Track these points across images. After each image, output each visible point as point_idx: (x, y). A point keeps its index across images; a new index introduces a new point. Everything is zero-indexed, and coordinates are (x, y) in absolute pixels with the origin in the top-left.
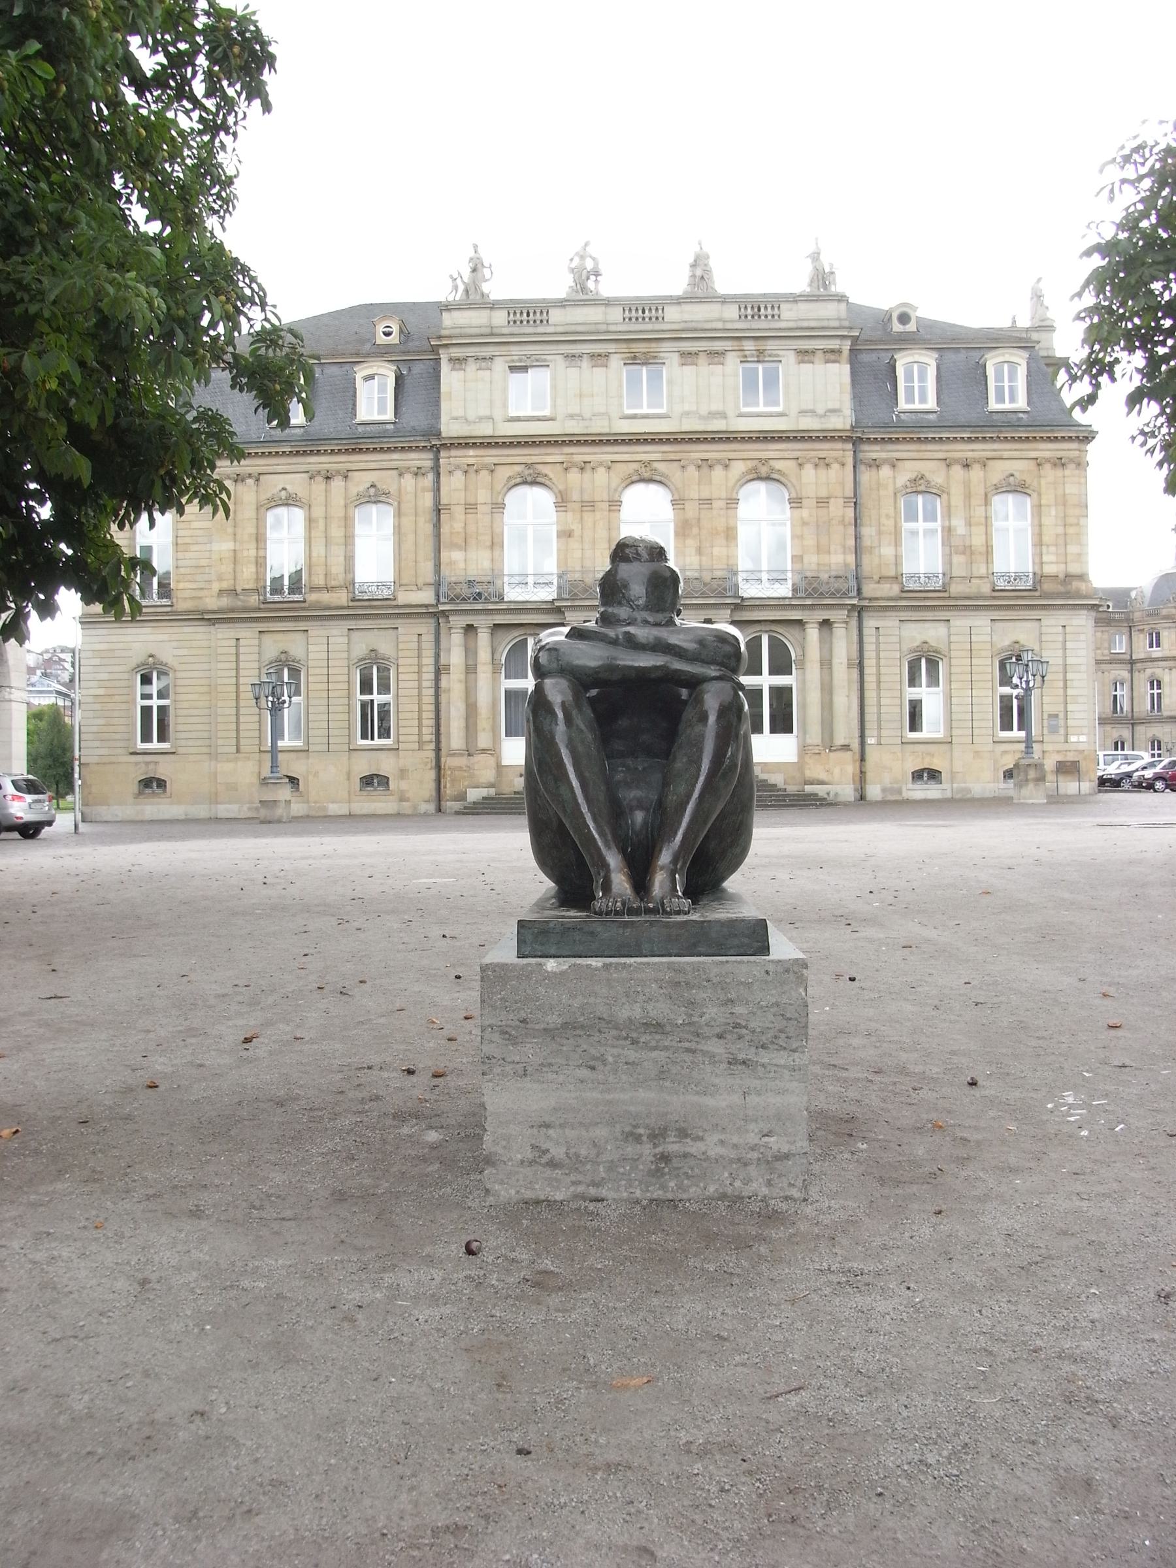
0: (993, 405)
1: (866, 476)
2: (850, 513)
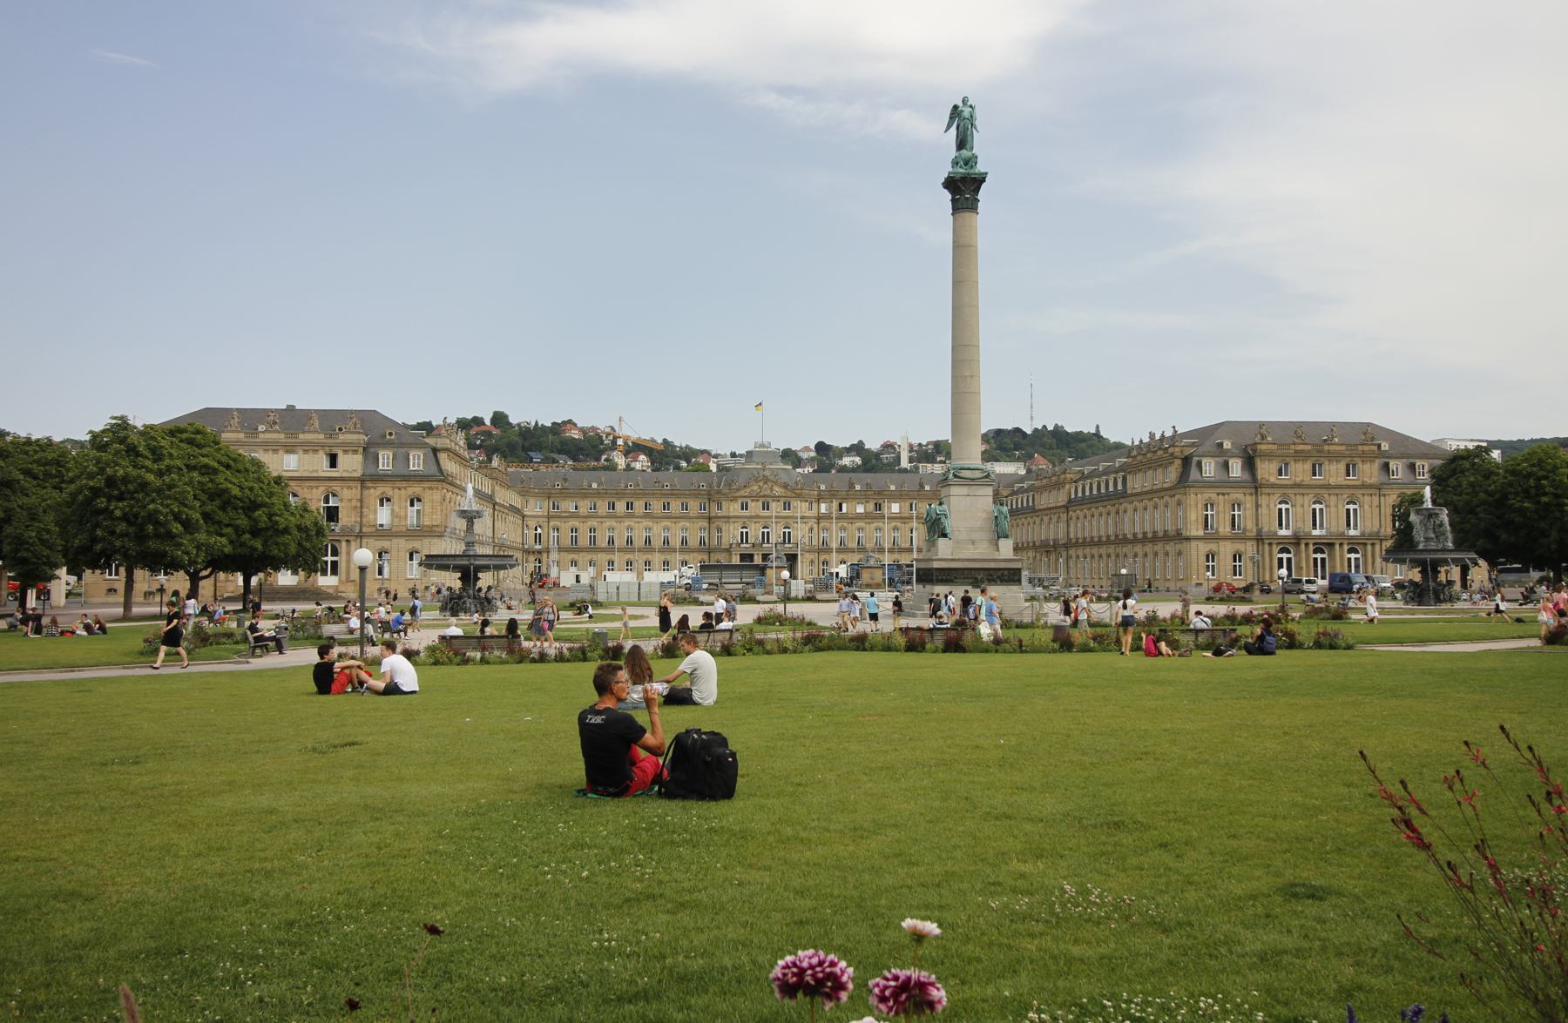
1: (366, 492)
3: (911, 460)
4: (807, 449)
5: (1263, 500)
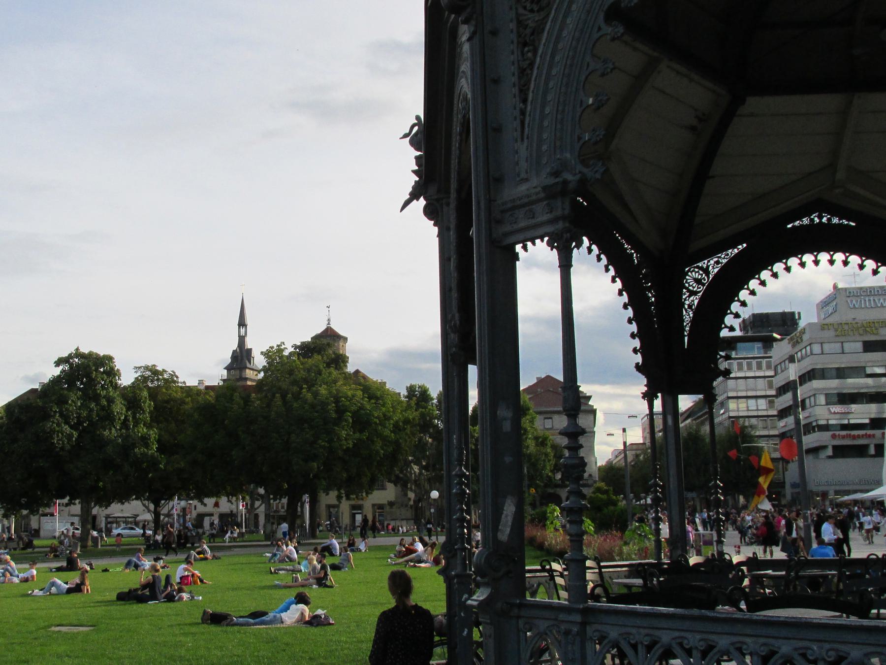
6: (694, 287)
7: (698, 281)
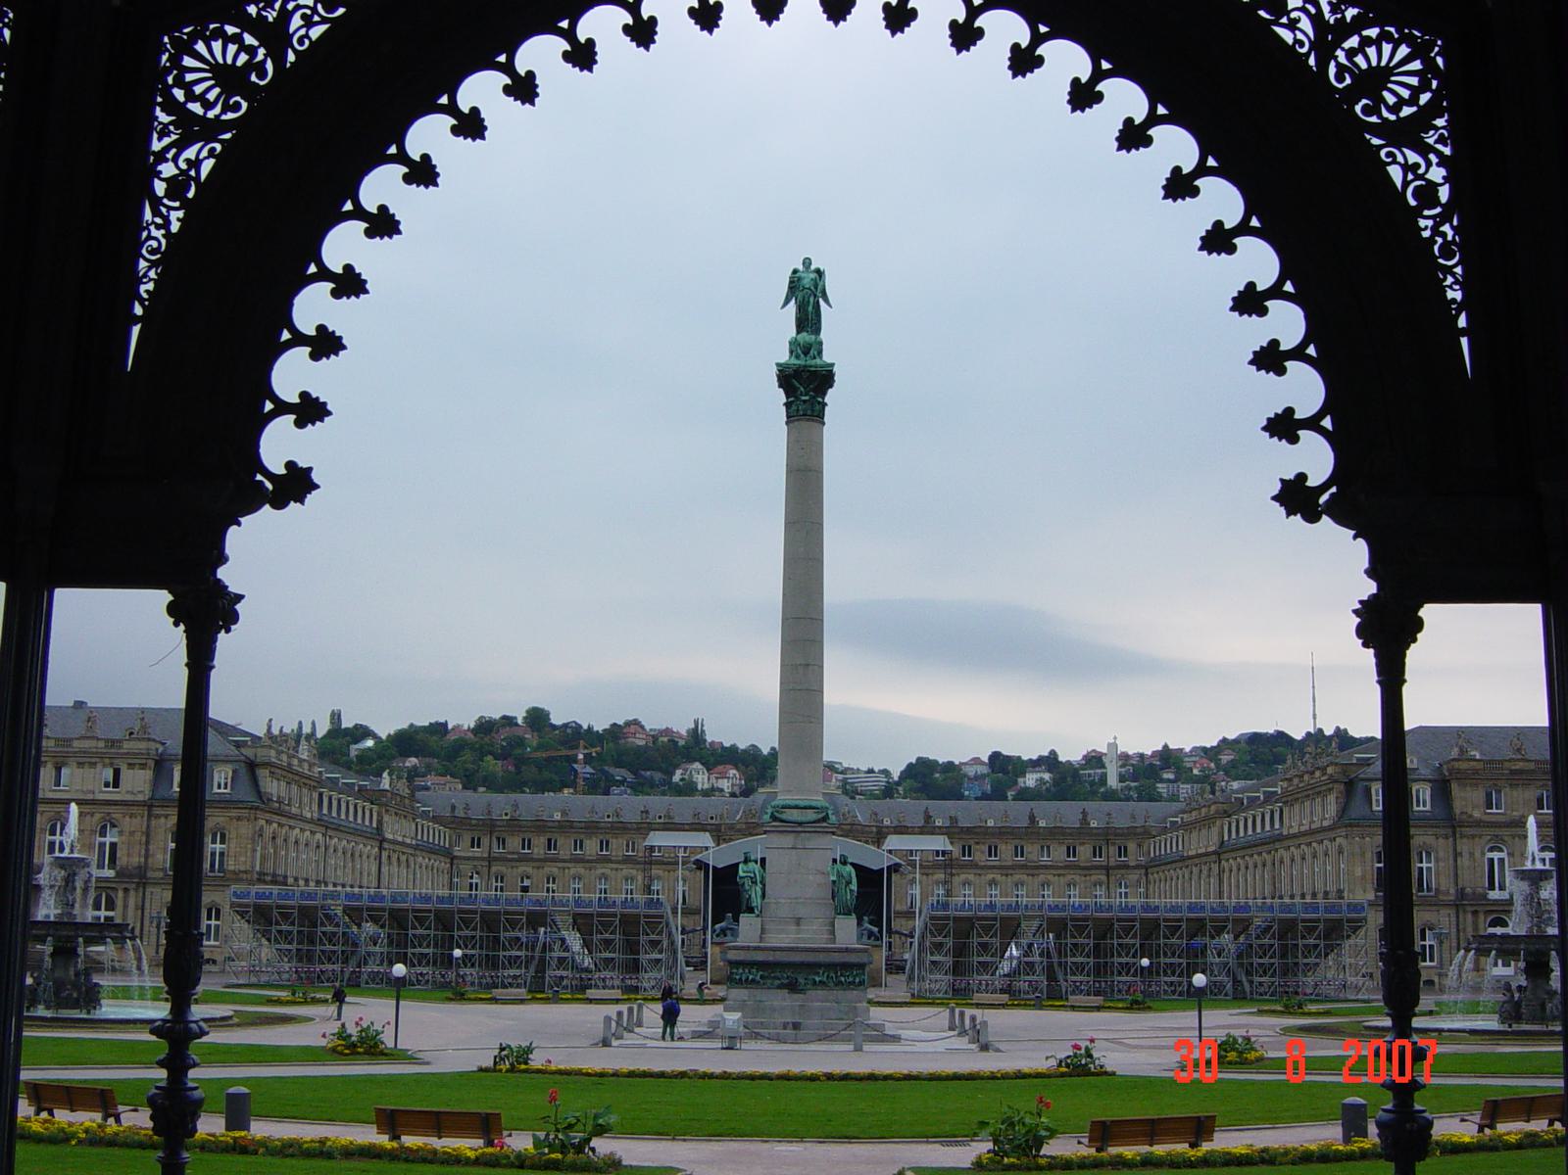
0: (216, 790)
2: (144, 839)
3: (1122, 778)
4: (976, 761)
5: (1464, 846)
6: (206, 99)
7: (228, 78)
